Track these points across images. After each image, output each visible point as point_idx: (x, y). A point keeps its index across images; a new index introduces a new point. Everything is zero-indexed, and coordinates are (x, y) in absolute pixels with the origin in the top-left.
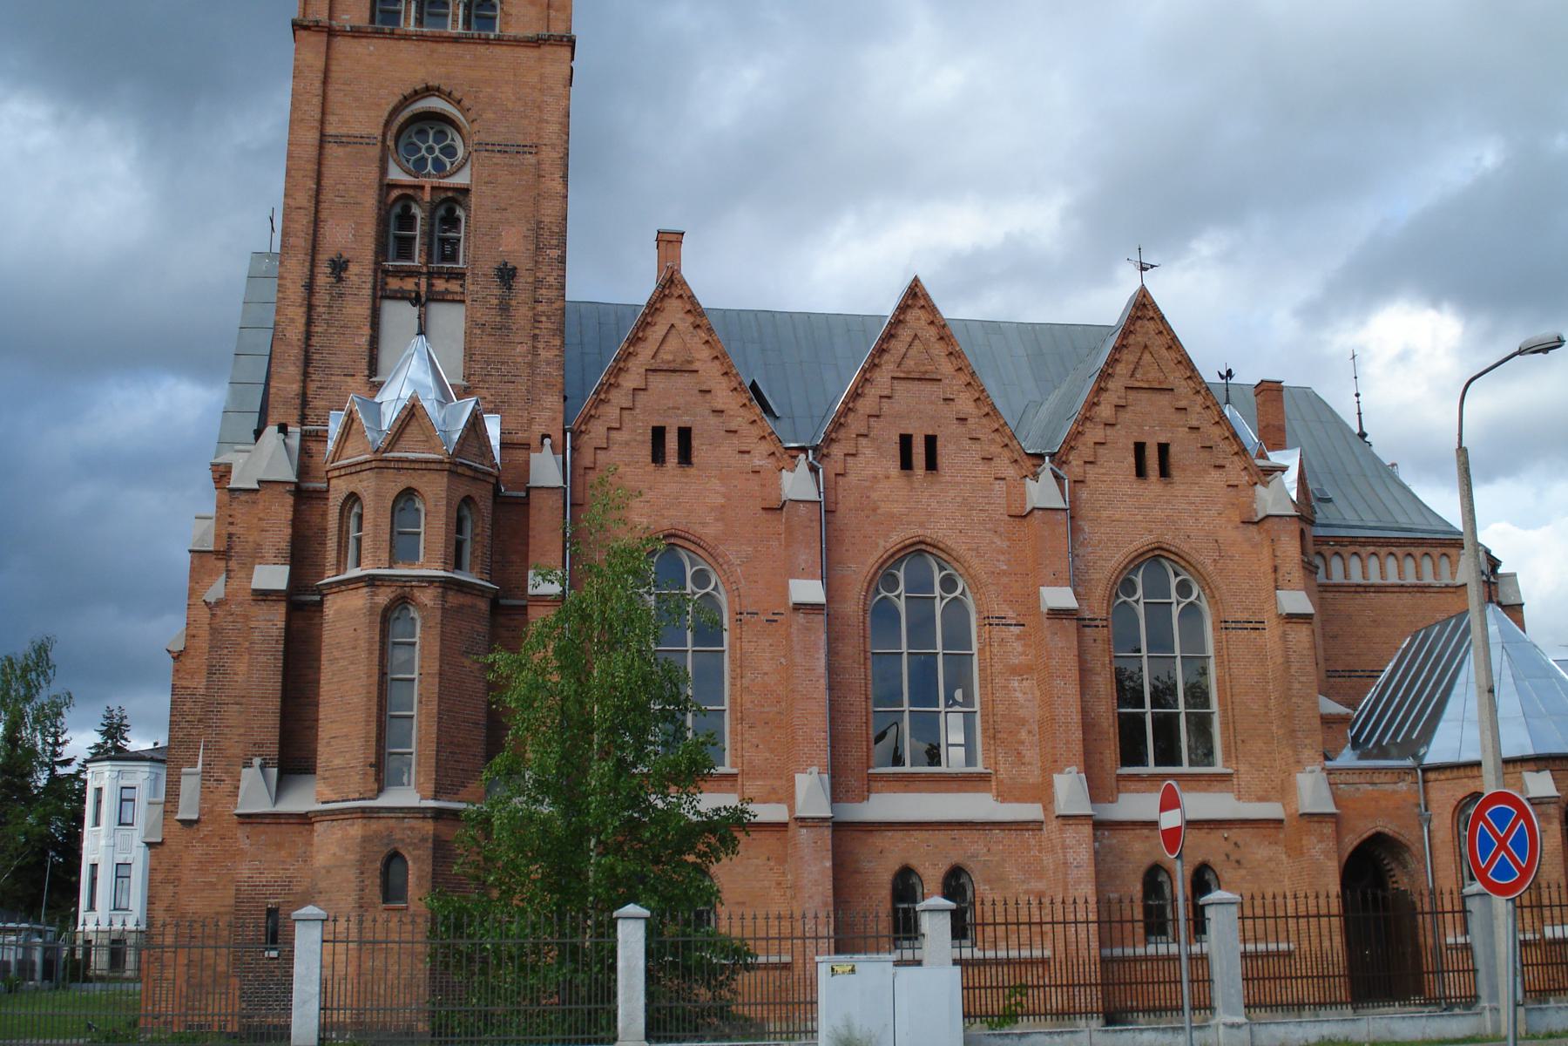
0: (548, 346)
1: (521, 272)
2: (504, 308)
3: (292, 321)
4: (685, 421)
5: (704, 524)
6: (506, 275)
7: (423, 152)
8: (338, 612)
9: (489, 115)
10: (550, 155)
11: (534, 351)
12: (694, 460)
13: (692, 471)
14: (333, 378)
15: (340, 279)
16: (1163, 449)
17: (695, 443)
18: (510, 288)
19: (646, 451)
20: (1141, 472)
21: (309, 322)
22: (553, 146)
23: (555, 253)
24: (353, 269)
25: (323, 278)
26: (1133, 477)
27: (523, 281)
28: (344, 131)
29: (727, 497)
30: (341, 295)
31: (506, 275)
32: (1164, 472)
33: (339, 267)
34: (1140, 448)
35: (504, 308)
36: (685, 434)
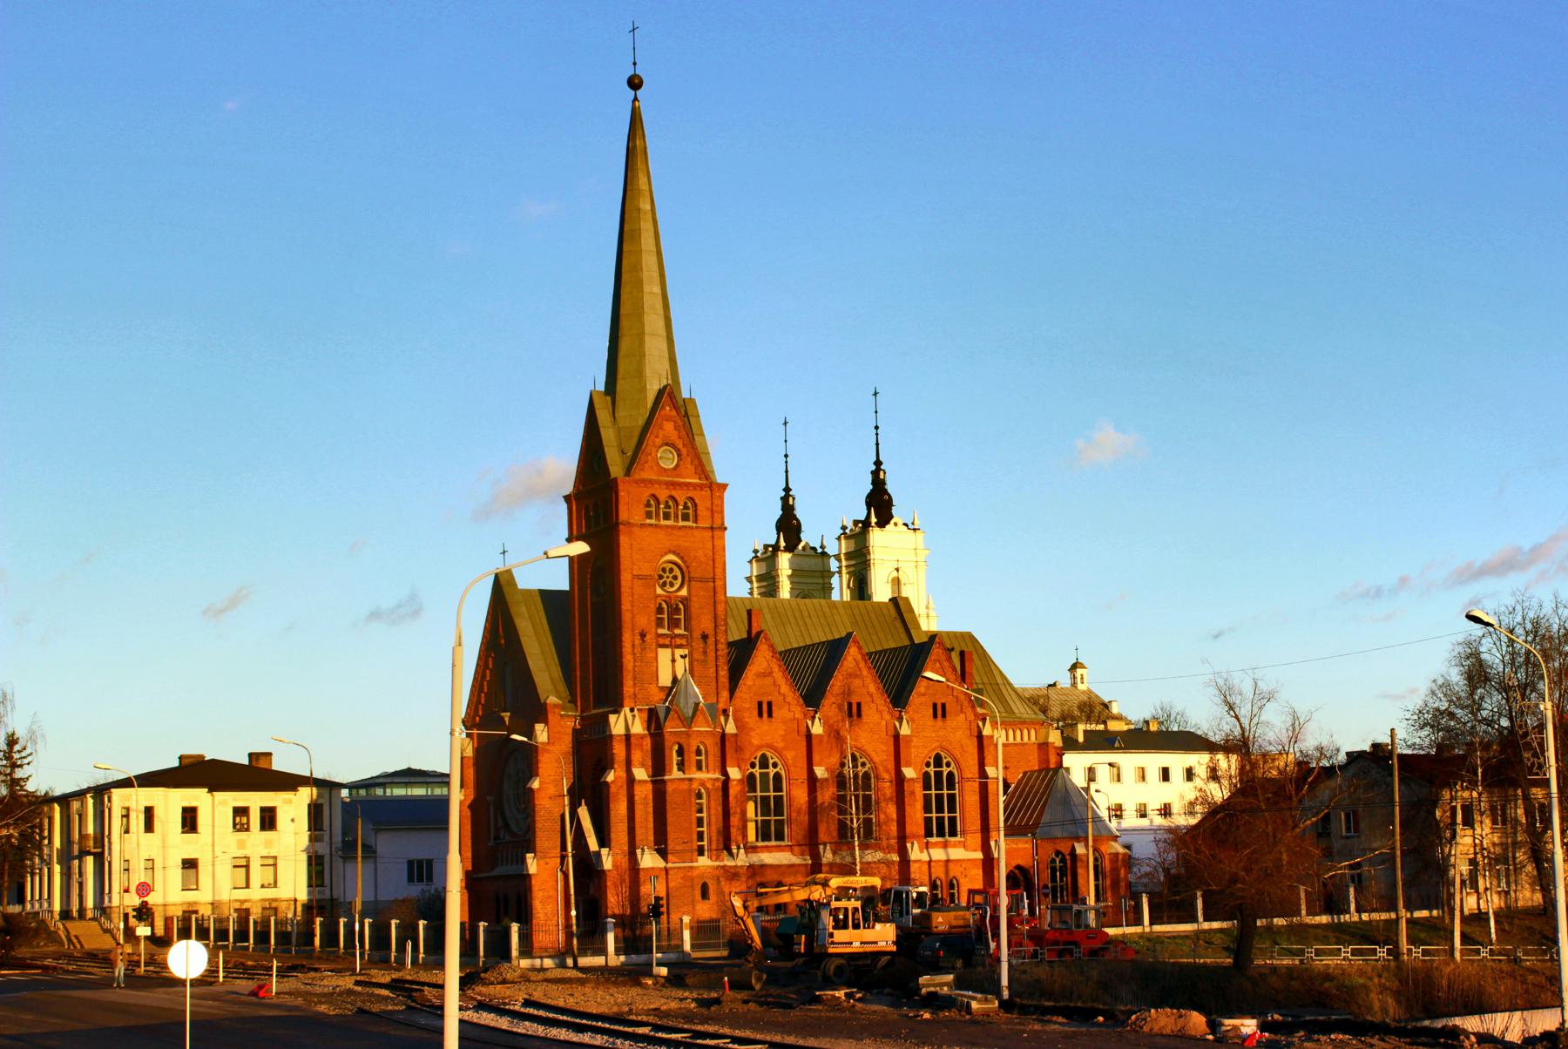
0: (723, 670)
1: (710, 636)
2: (705, 653)
3: (629, 661)
4: (769, 699)
5: (777, 742)
6: (705, 637)
7: (665, 575)
8: (674, 790)
9: (694, 564)
10: (719, 583)
11: (717, 671)
12: (773, 715)
13: (773, 720)
14: (646, 685)
15: (644, 641)
16: (943, 705)
17: (774, 708)
18: (706, 643)
19: (756, 712)
20: (935, 716)
21: (635, 661)
22: (720, 579)
23: (723, 628)
24: (648, 637)
25: (637, 642)
26: (932, 718)
27: (711, 640)
28: (640, 573)
29: (785, 730)
30: (645, 648)
31: (705, 637)
32: (944, 715)
33: (643, 635)
34: (935, 706)
35: (705, 653)
36: (770, 704)
